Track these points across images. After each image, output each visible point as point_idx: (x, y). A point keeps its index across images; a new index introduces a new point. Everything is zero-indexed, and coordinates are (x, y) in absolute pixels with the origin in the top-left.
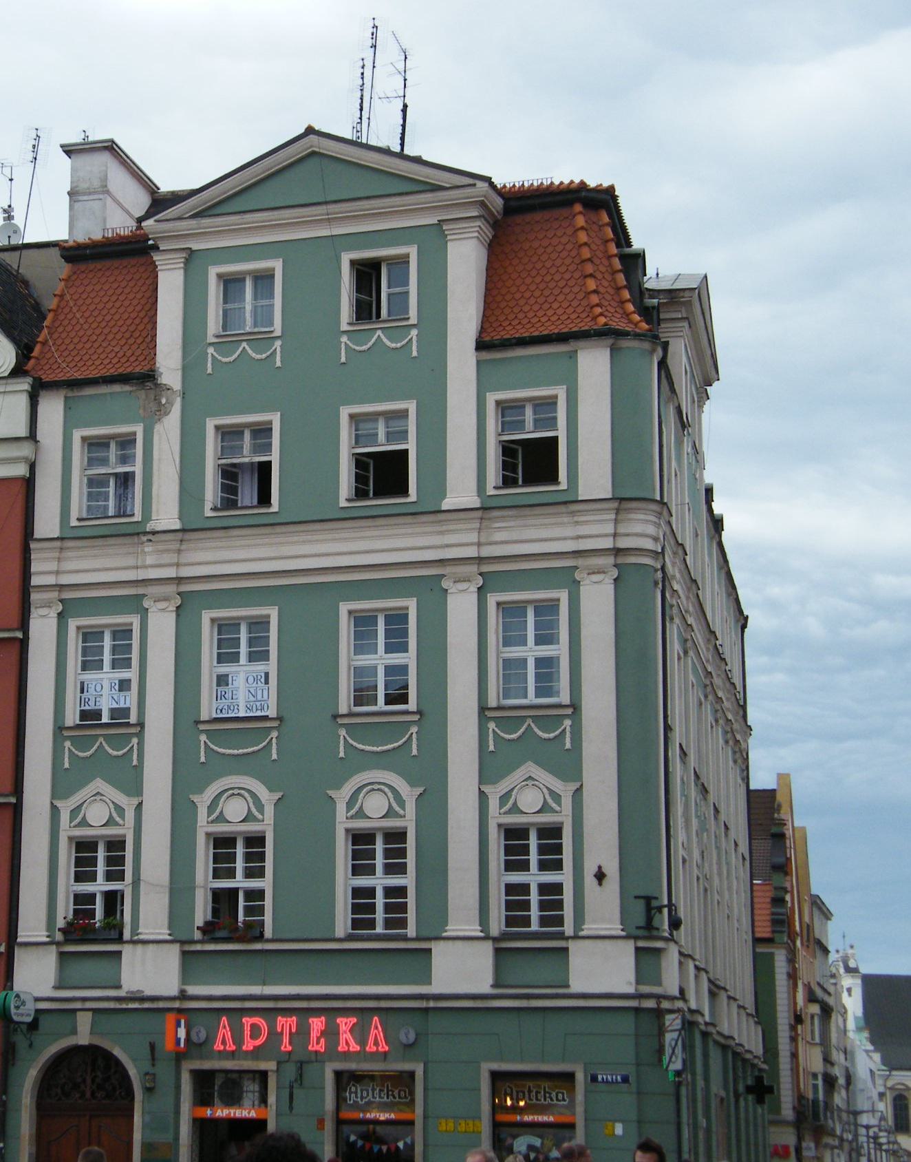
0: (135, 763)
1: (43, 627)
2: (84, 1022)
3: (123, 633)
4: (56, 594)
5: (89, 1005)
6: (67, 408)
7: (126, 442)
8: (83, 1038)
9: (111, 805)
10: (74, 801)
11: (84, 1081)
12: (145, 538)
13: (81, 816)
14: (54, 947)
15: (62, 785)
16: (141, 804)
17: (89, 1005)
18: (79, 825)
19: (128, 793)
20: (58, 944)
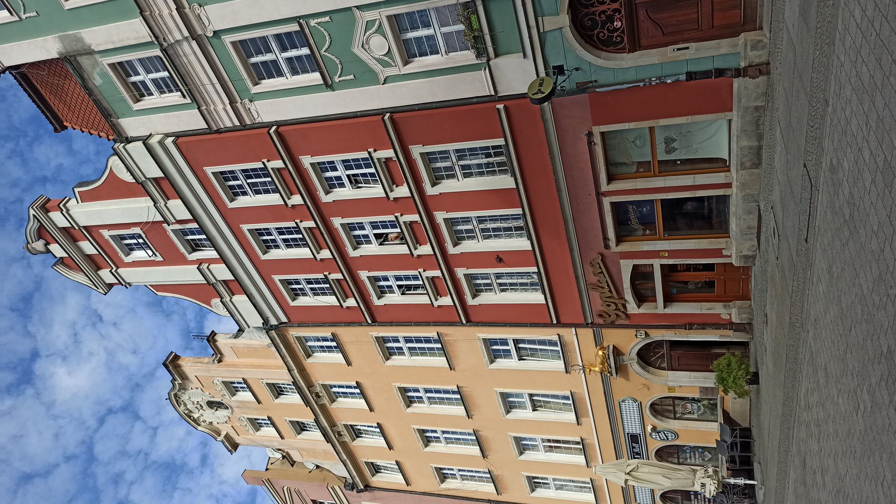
0: (327, 19)
1: (268, 111)
2: (549, 23)
3: (245, 48)
4: (239, 105)
5: (532, 23)
6: (124, 116)
7: (123, 70)
8: (564, 19)
9: (367, 34)
10: (377, 67)
11: (604, 12)
12: (165, 44)
13: (386, 58)
14: (491, 63)
15: (365, 76)
16: (357, 7)
17: (532, 23)
18: (392, 58)
19: (353, 20)
20: (489, 60)
